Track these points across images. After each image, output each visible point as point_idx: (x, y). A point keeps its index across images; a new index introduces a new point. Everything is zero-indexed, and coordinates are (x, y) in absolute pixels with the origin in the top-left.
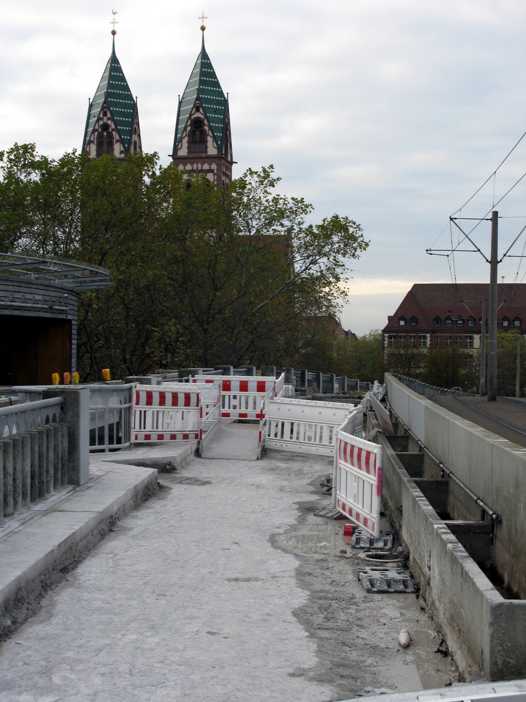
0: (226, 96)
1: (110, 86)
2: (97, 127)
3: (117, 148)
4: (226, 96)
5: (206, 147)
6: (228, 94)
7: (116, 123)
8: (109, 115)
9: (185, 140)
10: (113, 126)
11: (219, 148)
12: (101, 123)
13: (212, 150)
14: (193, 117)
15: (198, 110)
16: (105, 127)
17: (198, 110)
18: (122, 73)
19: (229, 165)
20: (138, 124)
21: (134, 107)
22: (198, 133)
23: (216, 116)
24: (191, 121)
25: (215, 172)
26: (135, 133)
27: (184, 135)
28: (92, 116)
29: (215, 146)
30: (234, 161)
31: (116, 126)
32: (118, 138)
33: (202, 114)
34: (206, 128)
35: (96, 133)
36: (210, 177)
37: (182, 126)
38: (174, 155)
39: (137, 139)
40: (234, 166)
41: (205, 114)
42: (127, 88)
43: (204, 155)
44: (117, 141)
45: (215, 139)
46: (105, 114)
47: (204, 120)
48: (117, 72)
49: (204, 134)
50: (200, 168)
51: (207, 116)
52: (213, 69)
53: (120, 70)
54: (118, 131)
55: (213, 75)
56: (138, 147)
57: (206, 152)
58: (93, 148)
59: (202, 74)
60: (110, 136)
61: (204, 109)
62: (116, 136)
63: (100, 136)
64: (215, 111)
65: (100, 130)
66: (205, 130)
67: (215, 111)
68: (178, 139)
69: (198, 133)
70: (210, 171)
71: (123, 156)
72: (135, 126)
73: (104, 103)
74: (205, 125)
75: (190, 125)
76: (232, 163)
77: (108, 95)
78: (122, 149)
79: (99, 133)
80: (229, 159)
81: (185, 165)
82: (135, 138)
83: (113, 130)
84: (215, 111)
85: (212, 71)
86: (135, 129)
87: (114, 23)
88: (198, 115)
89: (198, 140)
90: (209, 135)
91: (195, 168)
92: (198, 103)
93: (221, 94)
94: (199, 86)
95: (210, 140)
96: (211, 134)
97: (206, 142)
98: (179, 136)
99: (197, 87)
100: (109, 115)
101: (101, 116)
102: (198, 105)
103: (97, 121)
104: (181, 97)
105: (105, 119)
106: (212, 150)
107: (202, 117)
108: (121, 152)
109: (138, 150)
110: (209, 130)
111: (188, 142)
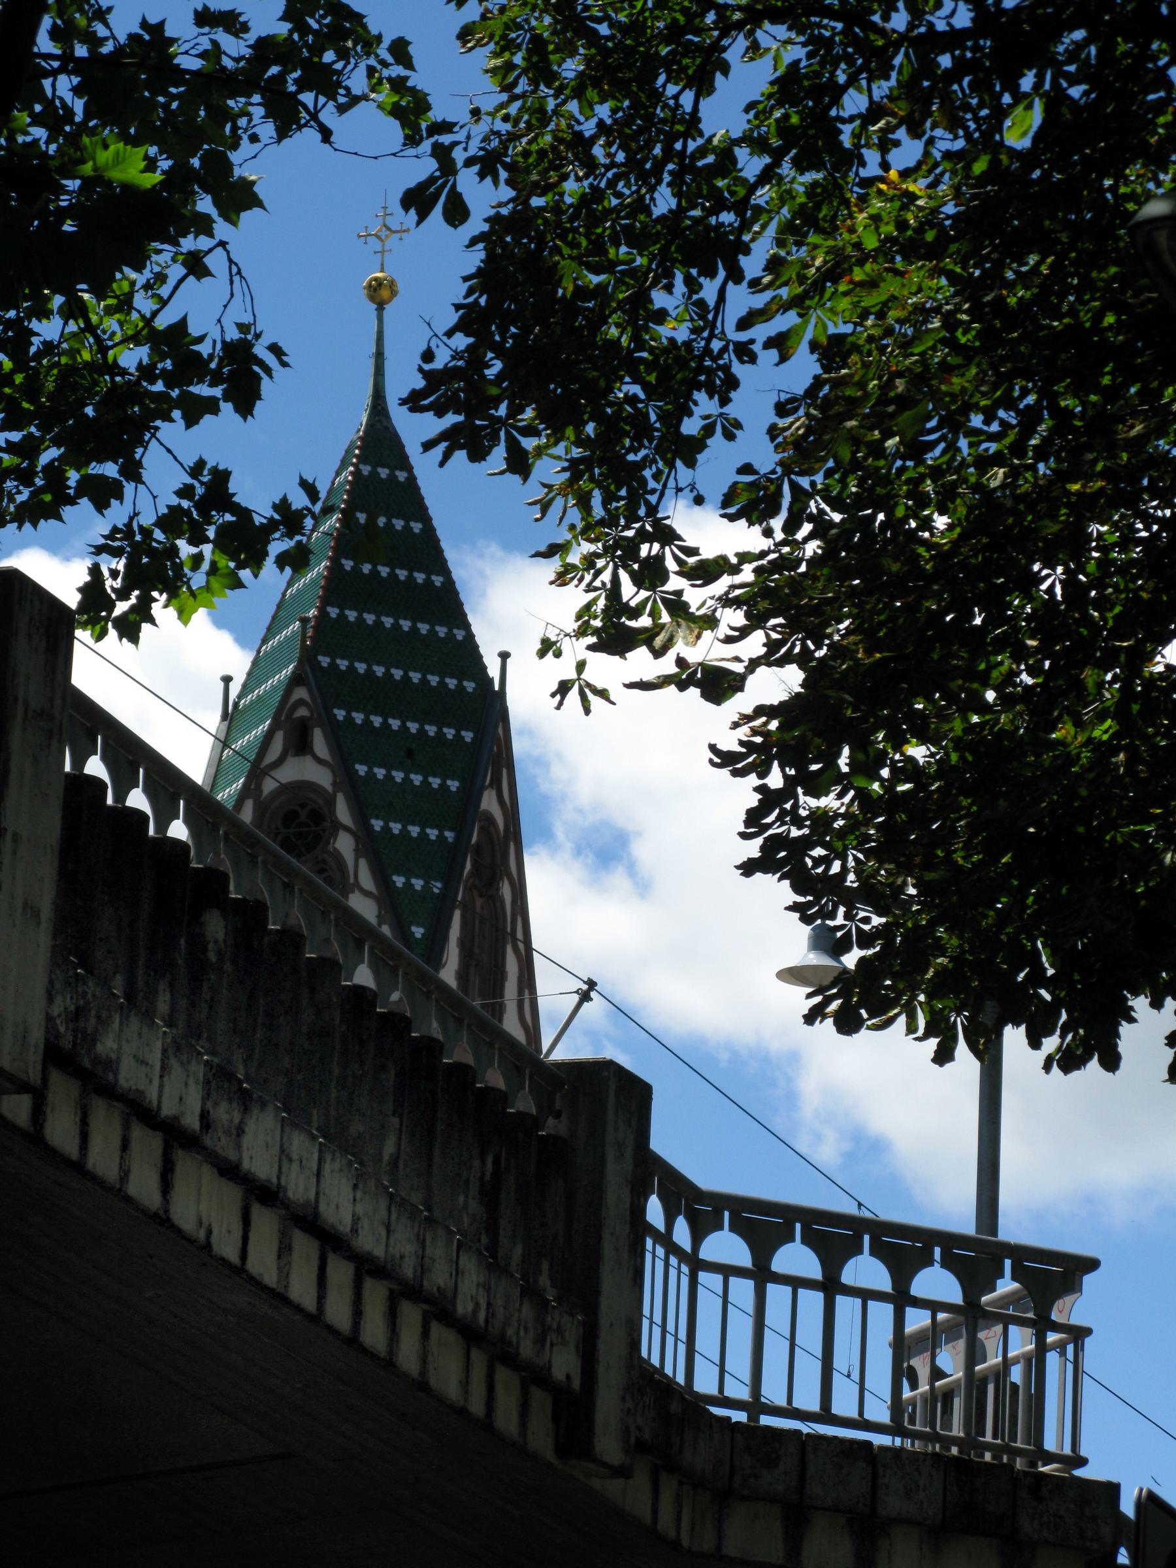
4: (493, 670)
6: (504, 656)
15: (300, 744)
17: (300, 744)
23: (417, 779)
33: (319, 761)
34: (344, 844)
41: (342, 765)
47: (331, 802)
51: (351, 774)
52: (426, 520)
61: (337, 733)
64: (410, 753)
66: (338, 858)
74: (337, 826)
85: (417, 527)
90: (357, 885)
92: (301, 702)
94: (322, 610)
96: (366, 879)
102: (302, 712)
107: (323, 777)
110: (358, 853)
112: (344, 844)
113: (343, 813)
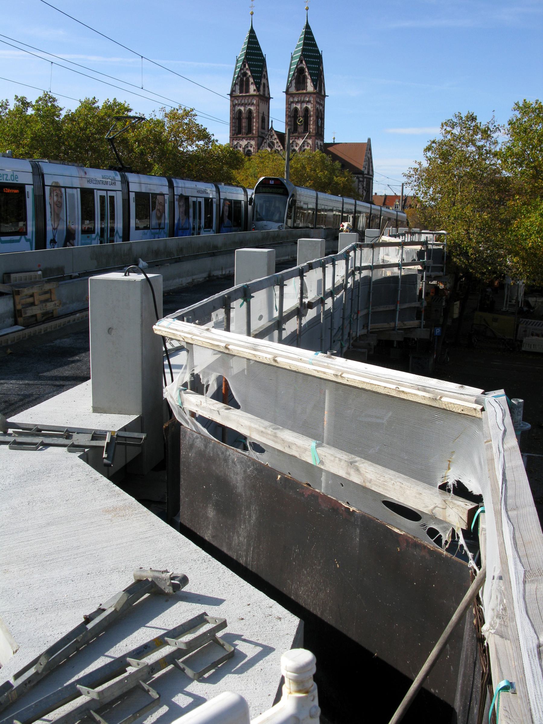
0: (321, 53)
1: (248, 48)
2: (240, 75)
3: (252, 88)
5: (307, 86)
7: (252, 72)
8: (247, 67)
9: (294, 82)
10: (249, 73)
11: (315, 87)
12: (242, 71)
13: (310, 88)
14: (299, 67)
16: (245, 74)
18: (257, 39)
19: (322, 98)
20: (266, 72)
21: (264, 61)
22: (301, 77)
24: (298, 70)
25: (312, 102)
26: (264, 78)
27: (293, 78)
28: (237, 67)
29: (312, 85)
30: (326, 95)
31: (251, 73)
32: (252, 81)
34: (307, 74)
35: (239, 78)
36: (309, 106)
37: (292, 73)
38: (287, 92)
39: (265, 82)
40: (326, 99)
42: (259, 49)
43: (305, 91)
44: (252, 83)
45: (313, 81)
46: (245, 66)
48: (253, 39)
49: (305, 78)
50: (302, 100)
53: (255, 37)
54: (254, 78)
55: (313, 39)
56: (266, 86)
57: (307, 90)
58: (238, 87)
59: (305, 39)
60: (248, 80)
61: (306, 61)
62: (251, 80)
63: (242, 80)
65: (242, 76)
67: (313, 63)
68: (289, 82)
69: (301, 77)
70: (309, 102)
71: (255, 93)
72: (264, 73)
73: (244, 59)
75: (297, 72)
76: (325, 96)
77: (247, 54)
78: (255, 88)
79: (241, 78)
80: (323, 94)
81: (293, 98)
82: (263, 81)
83: (250, 76)
84: (313, 63)
86: (264, 75)
87: (252, 7)
88: (301, 66)
89: (301, 81)
91: (300, 100)
93: (318, 51)
95: (309, 81)
96: (309, 77)
97: (307, 83)
98: (290, 79)
99: (302, 47)
100: (247, 67)
101: (242, 67)
103: (240, 71)
104: (293, 54)
105: (245, 69)
106: (310, 88)
108: (254, 90)
109: (266, 89)
111: (295, 83)
112: (307, 74)
113: (306, 70)
